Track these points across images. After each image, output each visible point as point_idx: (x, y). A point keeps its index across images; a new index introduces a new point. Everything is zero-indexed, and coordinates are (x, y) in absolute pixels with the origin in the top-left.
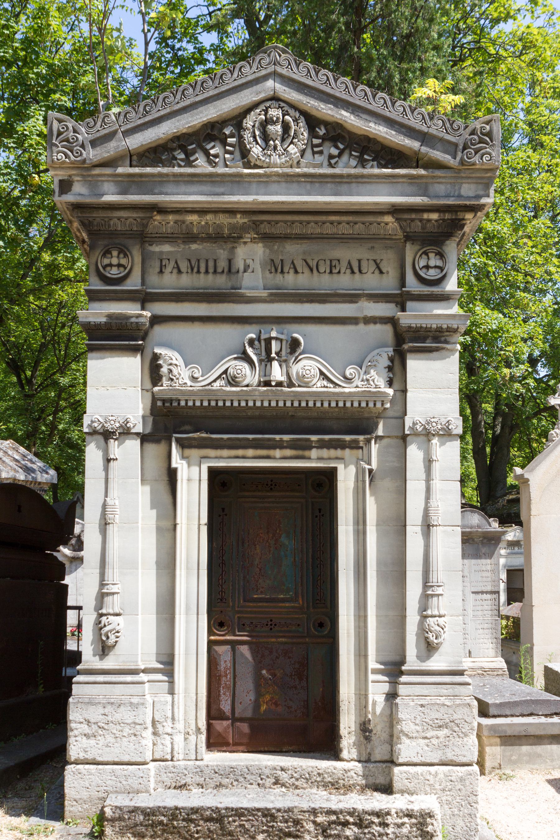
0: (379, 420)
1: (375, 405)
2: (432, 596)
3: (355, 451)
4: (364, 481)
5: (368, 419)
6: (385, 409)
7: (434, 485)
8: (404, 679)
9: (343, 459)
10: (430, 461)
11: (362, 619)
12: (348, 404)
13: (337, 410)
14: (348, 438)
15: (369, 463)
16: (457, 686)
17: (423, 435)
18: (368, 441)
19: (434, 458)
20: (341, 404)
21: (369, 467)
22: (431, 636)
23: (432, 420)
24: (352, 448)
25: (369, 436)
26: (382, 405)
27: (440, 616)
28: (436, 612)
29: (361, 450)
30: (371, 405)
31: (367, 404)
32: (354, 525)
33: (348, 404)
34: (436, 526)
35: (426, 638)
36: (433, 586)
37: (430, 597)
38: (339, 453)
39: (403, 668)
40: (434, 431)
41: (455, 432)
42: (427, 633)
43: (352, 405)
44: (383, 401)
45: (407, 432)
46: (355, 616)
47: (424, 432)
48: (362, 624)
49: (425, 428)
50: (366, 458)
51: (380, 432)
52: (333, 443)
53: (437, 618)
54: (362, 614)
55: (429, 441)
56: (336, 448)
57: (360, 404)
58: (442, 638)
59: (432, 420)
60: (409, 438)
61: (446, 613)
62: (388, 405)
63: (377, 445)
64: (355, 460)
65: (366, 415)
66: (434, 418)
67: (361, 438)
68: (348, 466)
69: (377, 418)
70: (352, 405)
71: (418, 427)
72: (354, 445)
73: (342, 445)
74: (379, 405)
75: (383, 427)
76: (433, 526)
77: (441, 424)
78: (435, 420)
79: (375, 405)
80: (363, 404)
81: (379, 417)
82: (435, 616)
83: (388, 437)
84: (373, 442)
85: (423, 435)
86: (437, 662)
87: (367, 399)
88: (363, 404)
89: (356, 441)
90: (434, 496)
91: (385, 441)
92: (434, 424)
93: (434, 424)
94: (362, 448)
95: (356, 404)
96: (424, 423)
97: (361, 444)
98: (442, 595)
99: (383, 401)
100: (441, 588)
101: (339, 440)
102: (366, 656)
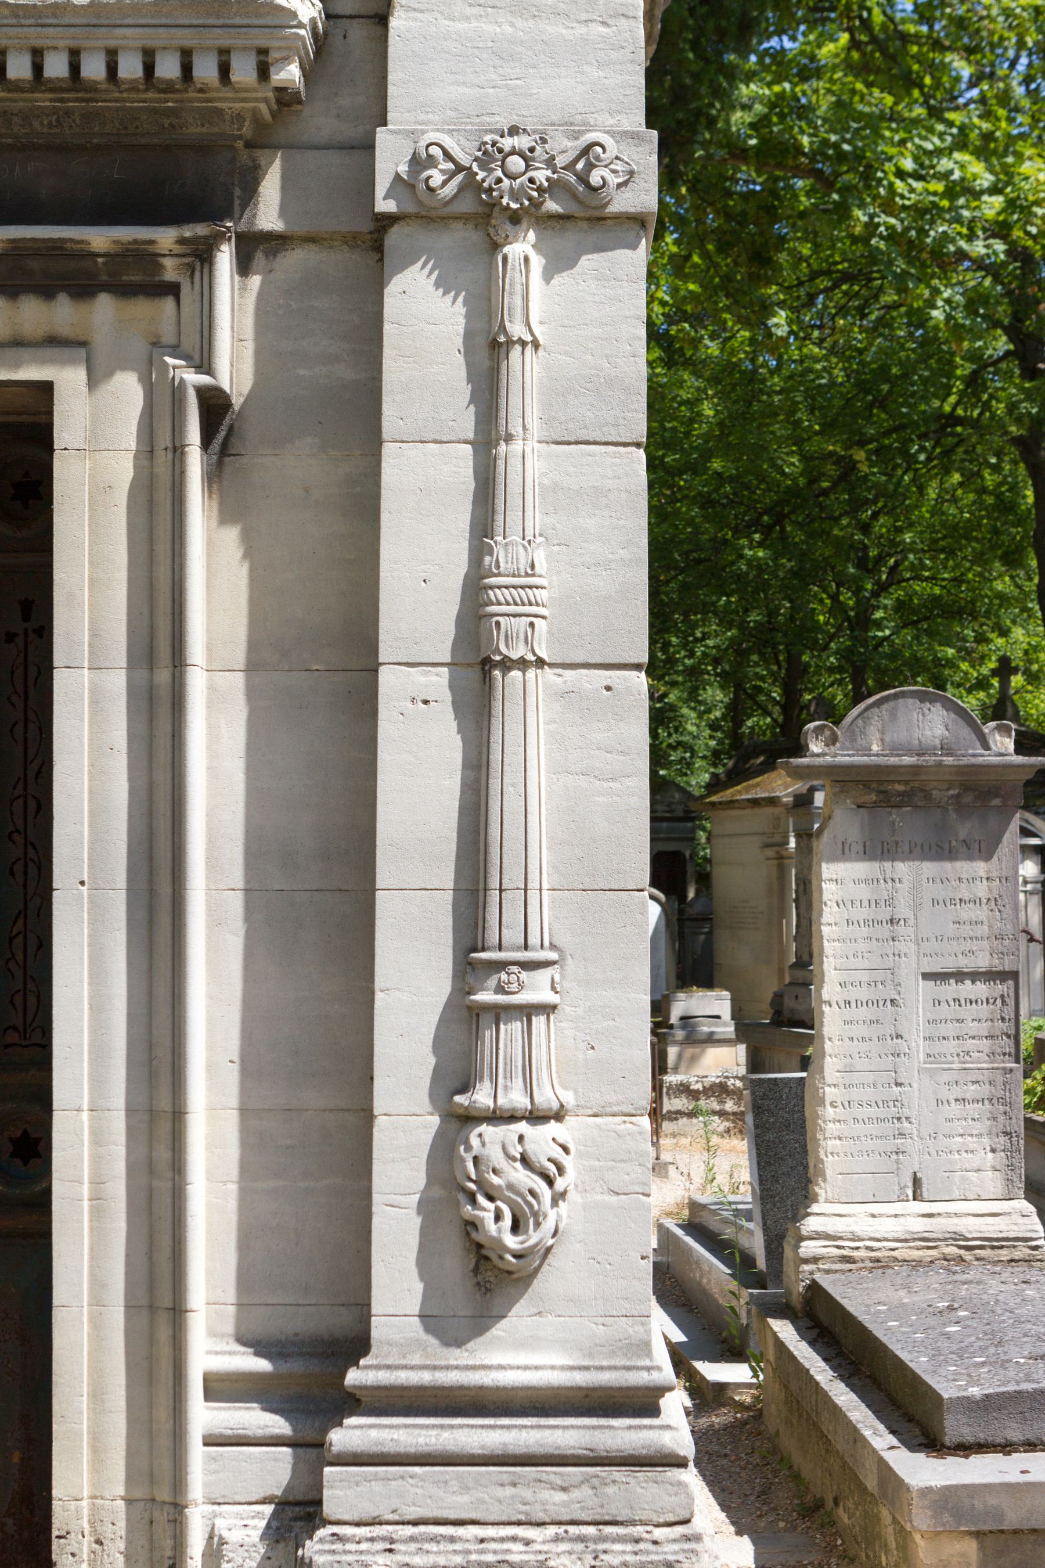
0: (262, 155)
1: (224, 70)
2: (499, 1013)
3: (140, 308)
4: (178, 451)
5: (203, 148)
6: (285, 98)
7: (515, 464)
8: (351, 1434)
9: (83, 344)
10: (494, 345)
11: (164, 1128)
12: (93, 69)
13: (43, 100)
14: (100, 238)
15: (204, 364)
16: (617, 1473)
17: (463, 218)
18: (201, 256)
19: (516, 330)
20: (56, 67)
21: (204, 379)
22: (489, 1217)
23: (507, 143)
24: (125, 291)
25: (201, 230)
26: (264, 72)
27: (536, 1117)
28: (516, 1098)
29: (169, 303)
30: (206, 70)
31: (187, 69)
32: (131, 667)
33: (93, 69)
34: (523, 664)
35: (472, 1225)
36: (501, 966)
37: (486, 1019)
38: (63, 313)
39: (353, 1377)
40: (514, 195)
41: (622, 203)
42: (472, 1199)
43: (112, 69)
44: (263, 52)
45: (385, 205)
46: (130, 1111)
47: (467, 205)
48: (163, 1154)
49: (471, 185)
50: (191, 341)
51: (268, 213)
52: (34, 264)
53: (522, 1127)
54: (164, 1103)
55: (495, 246)
56: (47, 293)
57: (149, 69)
58: (549, 1225)
59: (507, 143)
60: (394, 237)
61: (569, 1098)
62: (291, 73)
63: (255, 281)
64: (139, 347)
65: (195, 130)
66: (514, 131)
67: (166, 238)
68: (109, 374)
69: (249, 145)
70: (112, 69)
71: (437, 178)
72: (136, 279)
73: (75, 278)
74: (243, 71)
75: (284, 189)
76: (507, 665)
77: (550, 162)
78: (522, 142)
79: (224, 70)
80: (168, 68)
81: (262, 140)
82: (512, 1117)
83: (311, 239)
84: (225, 258)
85: (463, 218)
86: (518, 1352)
87: (186, 38)
88: (168, 68)
89: (144, 257)
90: (514, 517)
91: (294, 260)
92: (516, 163)
93: (516, 163)
94: (173, 290)
95: (130, 68)
96: (465, 160)
97: (171, 270)
98: (547, 1009)
99: (263, 52)
100: (543, 976)
101: (55, 249)
102: (177, 1313)
